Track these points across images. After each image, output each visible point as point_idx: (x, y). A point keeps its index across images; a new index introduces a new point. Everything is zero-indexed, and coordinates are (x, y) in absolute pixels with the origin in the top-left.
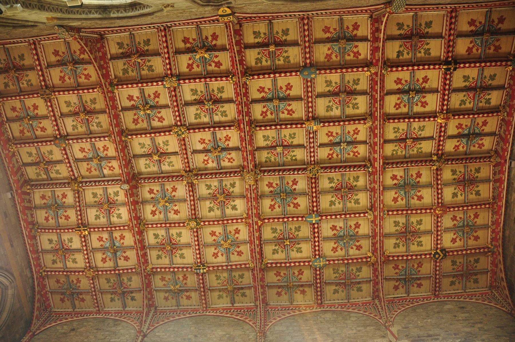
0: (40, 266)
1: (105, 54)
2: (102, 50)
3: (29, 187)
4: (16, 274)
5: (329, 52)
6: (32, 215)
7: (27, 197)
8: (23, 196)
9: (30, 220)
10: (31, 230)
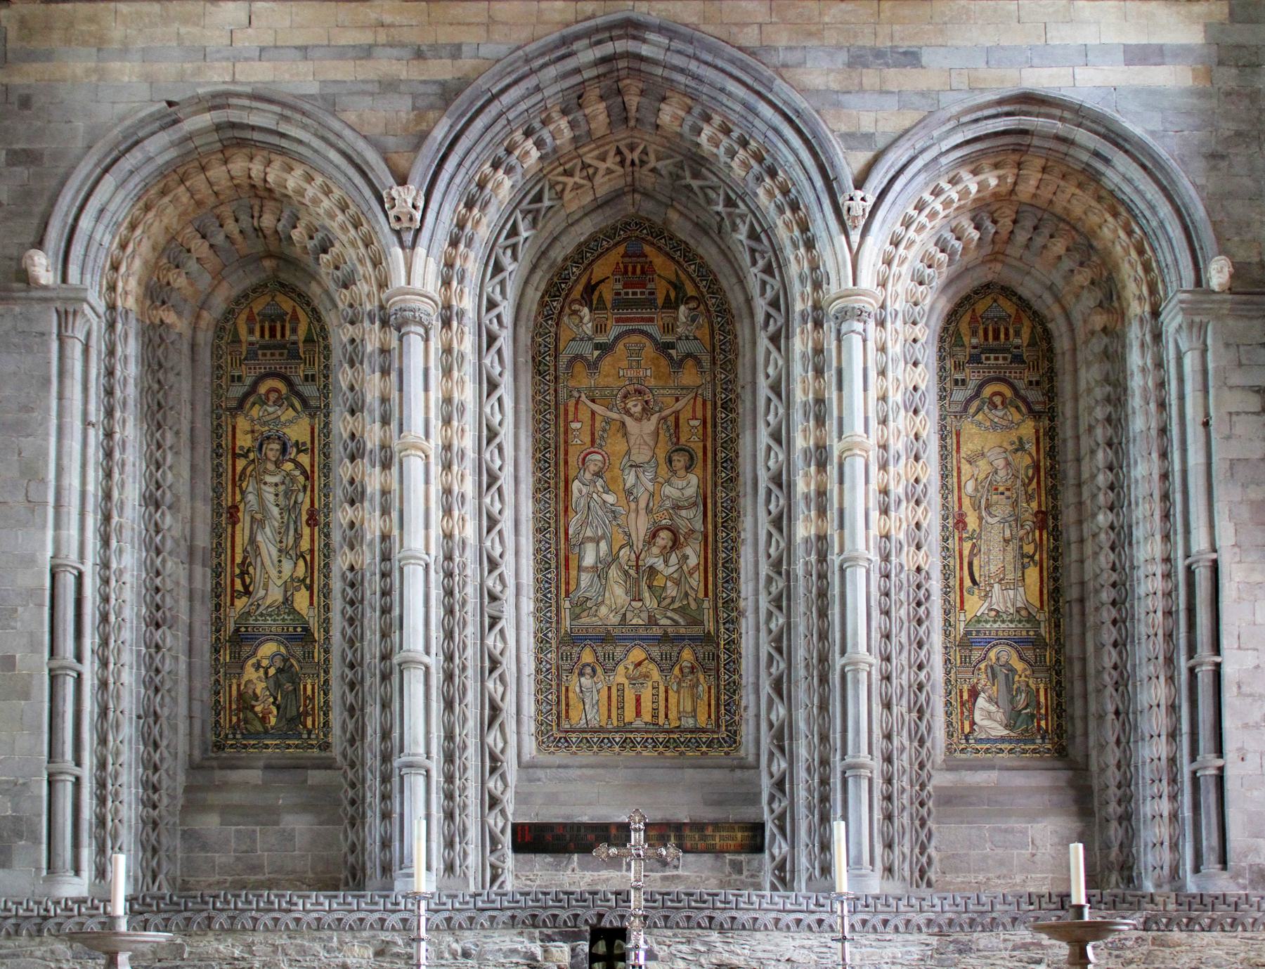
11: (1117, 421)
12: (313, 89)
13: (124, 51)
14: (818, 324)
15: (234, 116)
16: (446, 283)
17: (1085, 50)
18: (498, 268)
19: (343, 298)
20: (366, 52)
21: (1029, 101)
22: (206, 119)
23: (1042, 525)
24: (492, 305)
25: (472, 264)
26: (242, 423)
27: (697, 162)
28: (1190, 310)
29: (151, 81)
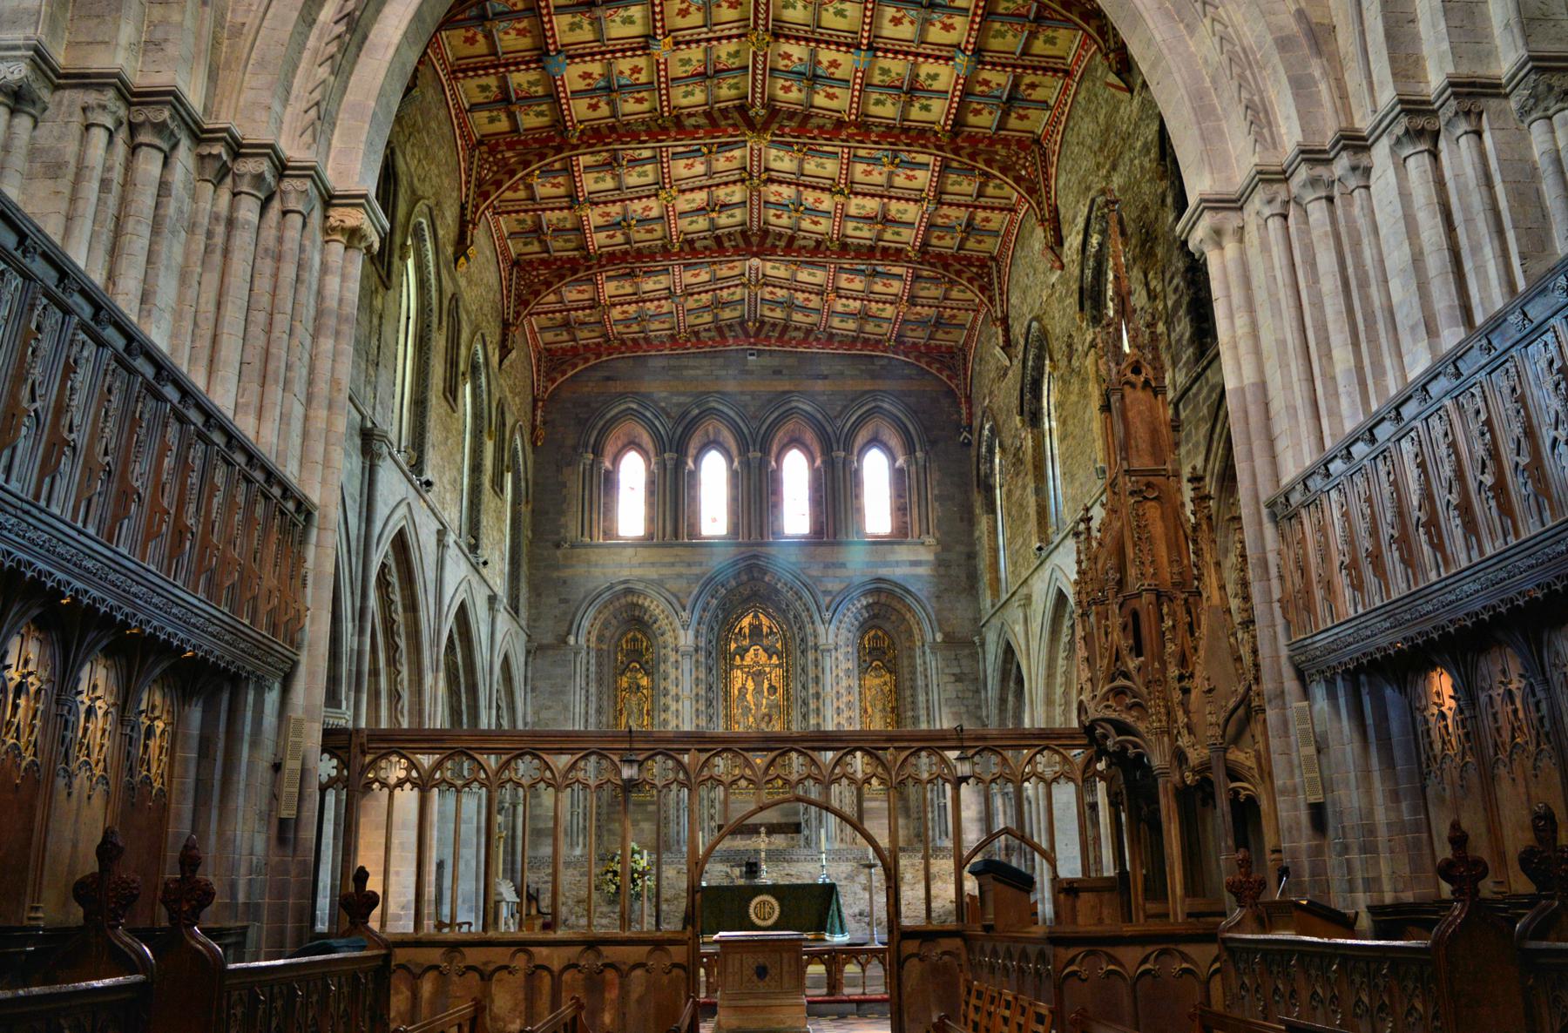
0: (878, 342)
1: (543, 262)
2: (536, 265)
3: (750, 324)
4: (868, 385)
5: (513, 33)
6: (797, 329)
7: (767, 327)
8: (762, 336)
9: (802, 335)
10: (817, 340)
11: (913, 680)
12: (655, 576)
13: (596, 565)
15: (630, 585)
16: (697, 637)
17: (897, 562)
18: (712, 629)
19: (661, 639)
20: (673, 564)
21: (879, 580)
22: (623, 586)
23: (893, 712)
24: (710, 642)
25: (704, 629)
26: (625, 679)
27: (777, 591)
28: (931, 648)
29: (604, 574)
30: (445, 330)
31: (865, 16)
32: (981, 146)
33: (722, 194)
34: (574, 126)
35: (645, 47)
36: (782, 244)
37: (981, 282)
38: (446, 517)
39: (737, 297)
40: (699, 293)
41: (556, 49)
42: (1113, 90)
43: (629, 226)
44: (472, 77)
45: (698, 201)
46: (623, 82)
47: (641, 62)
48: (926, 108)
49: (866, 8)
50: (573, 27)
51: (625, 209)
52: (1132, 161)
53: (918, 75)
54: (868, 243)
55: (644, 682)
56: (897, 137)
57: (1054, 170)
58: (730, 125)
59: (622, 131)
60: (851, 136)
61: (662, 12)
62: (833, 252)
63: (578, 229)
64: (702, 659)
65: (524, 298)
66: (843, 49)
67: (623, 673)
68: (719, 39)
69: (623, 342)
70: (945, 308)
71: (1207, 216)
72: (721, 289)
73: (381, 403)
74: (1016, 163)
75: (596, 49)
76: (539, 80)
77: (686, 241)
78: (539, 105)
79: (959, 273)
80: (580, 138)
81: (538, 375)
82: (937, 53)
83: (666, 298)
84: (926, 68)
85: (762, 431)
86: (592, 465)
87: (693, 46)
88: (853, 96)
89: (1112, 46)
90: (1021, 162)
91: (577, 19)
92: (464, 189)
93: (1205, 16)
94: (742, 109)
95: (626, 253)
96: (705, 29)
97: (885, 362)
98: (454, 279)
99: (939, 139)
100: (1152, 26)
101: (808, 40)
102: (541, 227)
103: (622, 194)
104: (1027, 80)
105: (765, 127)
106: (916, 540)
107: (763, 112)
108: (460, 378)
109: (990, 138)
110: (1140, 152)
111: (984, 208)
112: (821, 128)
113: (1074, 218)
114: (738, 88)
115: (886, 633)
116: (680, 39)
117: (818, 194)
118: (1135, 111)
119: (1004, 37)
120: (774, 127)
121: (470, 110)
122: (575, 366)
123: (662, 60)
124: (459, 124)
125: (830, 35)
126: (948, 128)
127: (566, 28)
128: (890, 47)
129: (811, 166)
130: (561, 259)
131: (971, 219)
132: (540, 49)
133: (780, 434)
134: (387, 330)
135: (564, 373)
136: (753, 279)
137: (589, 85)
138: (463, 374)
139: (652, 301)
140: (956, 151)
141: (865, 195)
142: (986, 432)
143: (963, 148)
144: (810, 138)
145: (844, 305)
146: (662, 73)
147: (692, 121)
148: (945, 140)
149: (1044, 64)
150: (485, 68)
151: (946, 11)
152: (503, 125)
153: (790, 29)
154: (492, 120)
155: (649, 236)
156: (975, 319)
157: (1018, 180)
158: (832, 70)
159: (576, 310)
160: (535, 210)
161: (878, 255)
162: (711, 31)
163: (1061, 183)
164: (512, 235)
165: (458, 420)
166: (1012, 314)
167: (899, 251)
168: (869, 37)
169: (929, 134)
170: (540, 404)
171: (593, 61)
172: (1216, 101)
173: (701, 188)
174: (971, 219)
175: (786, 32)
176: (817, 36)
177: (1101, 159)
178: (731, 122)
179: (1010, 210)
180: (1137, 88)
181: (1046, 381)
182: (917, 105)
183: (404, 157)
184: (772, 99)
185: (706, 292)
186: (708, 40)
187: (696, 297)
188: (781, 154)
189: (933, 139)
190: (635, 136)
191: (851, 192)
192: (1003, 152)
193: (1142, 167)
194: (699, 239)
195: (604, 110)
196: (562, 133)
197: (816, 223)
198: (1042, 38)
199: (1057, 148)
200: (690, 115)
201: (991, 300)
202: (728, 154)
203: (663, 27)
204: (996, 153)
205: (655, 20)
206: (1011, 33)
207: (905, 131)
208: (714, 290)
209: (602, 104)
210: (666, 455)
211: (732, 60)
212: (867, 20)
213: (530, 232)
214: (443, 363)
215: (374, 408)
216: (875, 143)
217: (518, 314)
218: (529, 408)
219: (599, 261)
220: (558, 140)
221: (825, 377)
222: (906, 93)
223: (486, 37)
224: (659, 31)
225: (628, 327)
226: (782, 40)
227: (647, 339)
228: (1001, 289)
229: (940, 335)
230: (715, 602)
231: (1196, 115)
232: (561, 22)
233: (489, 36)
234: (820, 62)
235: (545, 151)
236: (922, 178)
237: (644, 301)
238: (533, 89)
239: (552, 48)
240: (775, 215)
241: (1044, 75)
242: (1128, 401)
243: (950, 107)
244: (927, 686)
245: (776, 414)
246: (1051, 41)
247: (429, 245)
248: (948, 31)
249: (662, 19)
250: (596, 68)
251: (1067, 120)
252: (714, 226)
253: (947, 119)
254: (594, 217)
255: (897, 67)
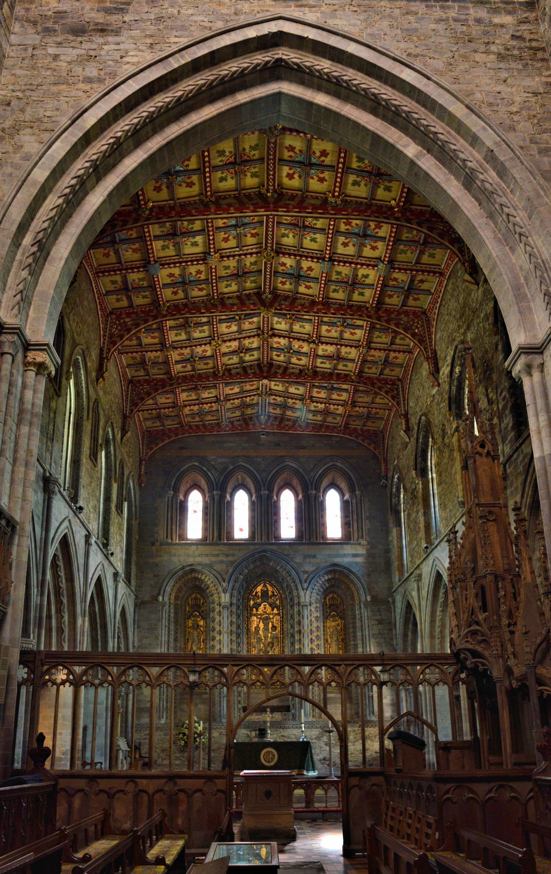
0: (335, 427)
1: (146, 381)
2: (142, 383)
3: (262, 417)
5: (130, 251)
6: (289, 420)
14: (299, 605)
17: (345, 555)
18: (240, 593)
20: (218, 555)
21: (335, 565)
25: (235, 593)
27: (277, 571)
29: (179, 561)
30: (90, 420)
31: (327, 241)
32: (393, 316)
33: (246, 342)
34: (164, 304)
35: (204, 259)
36: (281, 371)
37: (392, 394)
38: (90, 527)
39: (254, 402)
40: (234, 399)
41: (154, 260)
42: (467, 284)
43: (195, 361)
44: (107, 276)
45: (233, 347)
46: (192, 279)
47: (202, 268)
48: (362, 294)
49: (328, 237)
50: (164, 248)
51: (192, 351)
52: (478, 324)
53: (357, 275)
54: (329, 371)
55: (201, 623)
56: (345, 310)
57: (434, 329)
58: (252, 304)
59: (191, 306)
60: (319, 311)
61: (213, 239)
62: (309, 377)
63: (166, 363)
64: (234, 610)
65: (135, 401)
66: (315, 260)
67: (189, 618)
68: (245, 255)
69: (191, 427)
70: (372, 408)
71: (523, 356)
72: (246, 397)
73: (55, 462)
74: (412, 325)
75: (177, 260)
76: (145, 278)
77: (226, 369)
78: (144, 292)
79: (380, 388)
80: (167, 311)
81: (143, 446)
82: (368, 262)
83: (215, 402)
84: (362, 271)
85: (269, 479)
86: (172, 497)
87: (231, 258)
88: (320, 287)
89: (467, 258)
90: (415, 325)
91: (166, 243)
92: (102, 340)
93: (521, 242)
94: (258, 294)
95: (193, 376)
96: (238, 249)
97: (338, 439)
98: (96, 391)
99: (369, 312)
100: (490, 248)
101: (295, 255)
102: (145, 362)
103: (191, 343)
104: (419, 278)
105: (271, 305)
106: (356, 542)
107: (270, 296)
108: (99, 447)
109: (398, 311)
110: (483, 319)
111: (394, 351)
112: (302, 305)
113: (446, 357)
114: (256, 283)
115: (338, 596)
116: (224, 254)
117: (301, 343)
118: (480, 296)
119: (406, 254)
120: (276, 304)
121: (106, 295)
122: (163, 441)
123: (213, 267)
124: (100, 303)
125: (308, 253)
126: (374, 305)
127: (160, 248)
128: (341, 259)
129: (297, 327)
130: (156, 379)
131: (387, 357)
132: (146, 260)
133: (279, 480)
134: (59, 420)
135: (157, 444)
136: (264, 391)
137: (172, 280)
138: (101, 445)
139: (207, 404)
140: (379, 319)
141: (327, 343)
142: (396, 480)
143: (382, 317)
144: (296, 311)
145: (315, 407)
146: (214, 274)
147: (230, 301)
148: (372, 312)
149: (428, 269)
150: (115, 271)
151: (373, 238)
152: (125, 303)
153: (285, 249)
154: (118, 300)
155: (205, 367)
156: (389, 415)
157: (414, 335)
158: (309, 272)
159: (164, 408)
160: (142, 352)
161: (334, 378)
162: (241, 250)
163: (438, 337)
164: (129, 365)
165: (97, 472)
166: (410, 412)
167: (346, 376)
168: (330, 254)
169: (363, 309)
170: (144, 462)
171: (175, 267)
172: (527, 290)
173: (235, 340)
174: (387, 357)
175: (283, 250)
176: (300, 253)
177: (461, 323)
178: (252, 302)
179: (409, 352)
180: (481, 283)
181: (430, 450)
182: (357, 292)
183: (69, 321)
184: (275, 288)
185: (238, 399)
186: (240, 255)
187: (232, 401)
188: (280, 320)
189: (365, 312)
190: (198, 310)
191: (320, 342)
192: (405, 319)
193: (484, 327)
194: (234, 368)
195: (181, 295)
196: (157, 308)
197: (300, 360)
198: (427, 254)
199: (436, 317)
200: (229, 298)
201: (398, 404)
202: (250, 320)
203: (214, 247)
204: (401, 319)
205: (209, 244)
206: (409, 251)
207: (350, 307)
208: (242, 398)
209: (180, 292)
210: (215, 492)
211: (253, 267)
212: (329, 244)
213: (139, 364)
214: (89, 439)
215: (51, 465)
216: (333, 314)
217: (132, 411)
218: (137, 465)
219: (178, 381)
220: (155, 311)
221: (304, 448)
222: (350, 286)
223: (115, 253)
224: (212, 250)
225: (193, 419)
226: (281, 255)
227: (204, 426)
228: (404, 397)
229: (369, 423)
230: (242, 577)
231: (516, 299)
232: (157, 245)
233: (117, 253)
234: (302, 268)
235: (148, 318)
236: (359, 334)
237: (203, 404)
238: (141, 283)
239: (152, 259)
240: (276, 355)
241: (428, 275)
242: (478, 463)
243: (375, 294)
244: (362, 626)
245: (277, 469)
246: (432, 256)
247: (82, 372)
248: (374, 250)
249: (214, 243)
250: (176, 271)
251: (441, 300)
252: (242, 361)
253: (373, 300)
254: (175, 356)
255: (345, 270)
